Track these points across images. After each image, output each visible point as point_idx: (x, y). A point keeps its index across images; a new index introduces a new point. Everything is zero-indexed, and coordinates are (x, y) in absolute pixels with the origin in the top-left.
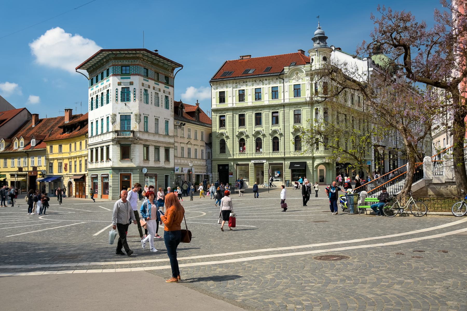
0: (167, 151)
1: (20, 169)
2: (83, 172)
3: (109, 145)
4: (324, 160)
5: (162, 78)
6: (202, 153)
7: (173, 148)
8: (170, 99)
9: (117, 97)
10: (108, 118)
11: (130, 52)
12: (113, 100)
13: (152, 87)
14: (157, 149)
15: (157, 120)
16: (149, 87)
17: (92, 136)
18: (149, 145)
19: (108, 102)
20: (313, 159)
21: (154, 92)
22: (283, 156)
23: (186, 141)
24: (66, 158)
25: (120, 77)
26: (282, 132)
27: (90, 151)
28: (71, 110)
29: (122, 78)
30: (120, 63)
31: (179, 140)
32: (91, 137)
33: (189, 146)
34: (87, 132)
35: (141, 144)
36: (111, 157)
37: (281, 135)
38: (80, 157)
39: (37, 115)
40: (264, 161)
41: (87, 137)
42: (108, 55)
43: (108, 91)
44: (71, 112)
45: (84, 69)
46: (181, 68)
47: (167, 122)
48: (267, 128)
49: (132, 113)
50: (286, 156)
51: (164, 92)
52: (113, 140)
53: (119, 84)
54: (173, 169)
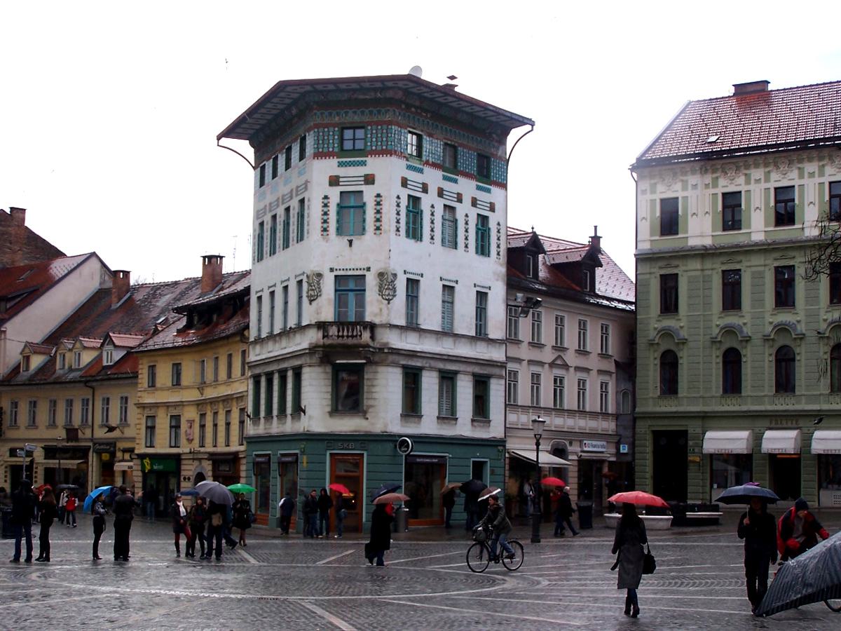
0: (481, 386)
1: (72, 433)
2: (235, 447)
5: (468, 159)
6: (604, 393)
7: (500, 377)
8: (492, 225)
9: (325, 222)
10: (300, 283)
13: (433, 190)
14: (448, 379)
15: (449, 290)
16: (425, 189)
17: (259, 341)
18: (421, 369)
19: (301, 238)
21: (440, 204)
23: (548, 355)
24: (190, 403)
25: (334, 162)
27: (251, 382)
29: (340, 165)
31: (524, 352)
33: (559, 372)
34: (247, 327)
35: (395, 364)
36: (304, 403)
38: (227, 399)
39: (126, 273)
41: (244, 339)
42: (304, 95)
43: (302, 201)
46: (528, 127)
47: (482, 297)
49: (368, 269)
51: (474, 203)
52: (313, 350)
53: (334, 181)
54: (498, 444)
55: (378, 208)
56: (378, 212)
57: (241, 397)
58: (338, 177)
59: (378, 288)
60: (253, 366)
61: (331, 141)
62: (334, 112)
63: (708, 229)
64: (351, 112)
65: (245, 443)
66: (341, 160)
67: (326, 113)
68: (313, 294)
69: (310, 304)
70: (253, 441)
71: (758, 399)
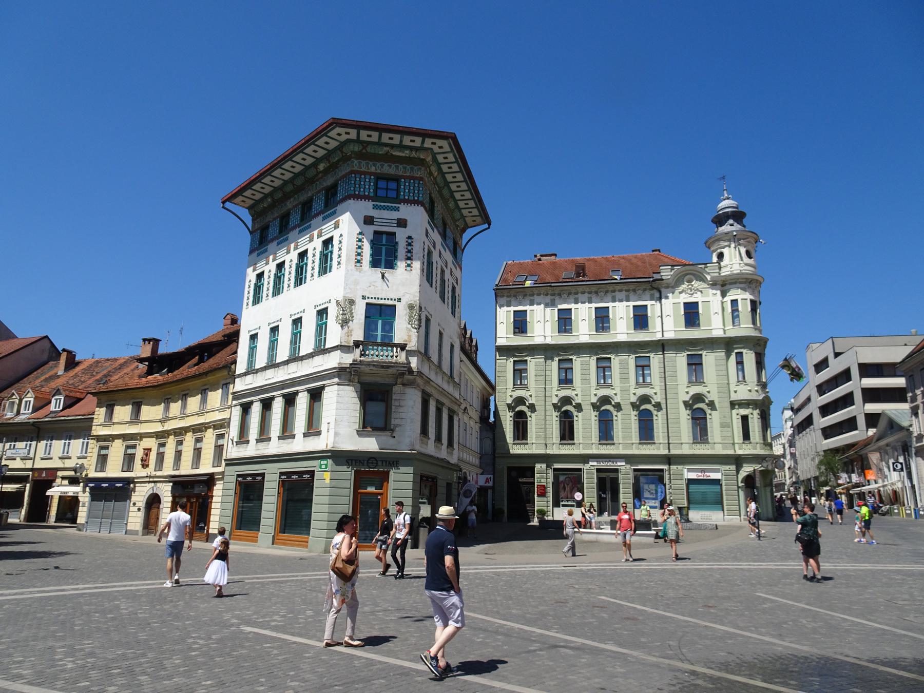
2: (206, 467)
3: (323, 388)
4: (765, 464)
11: (407, 141)
12: (348, 260)
20: (738, 461)
22: (666, 452)
24: (149, 435)
25: (370, 204)
26: (658, 398)
28: (156, 342)
29: (375, 207)
30: (373, 169)
32: (246, 374)
34: (235, 362)
37: (658, 406)
40: (621, 464)
43: (328, 243)
44: (158, 345)
45: (242, 204)
46: (486, 226)
48: (625, 391)
49: (399, 300)
50: (673, 452)
55: (409, 248)
56: (409, 251)
57: (223, 424)
58: (372, 218)
60: (236, 396)
63: (548, 333)
65: (223, 463)
67: (363, 162)
70: (231, 463)
71: (587, 445)
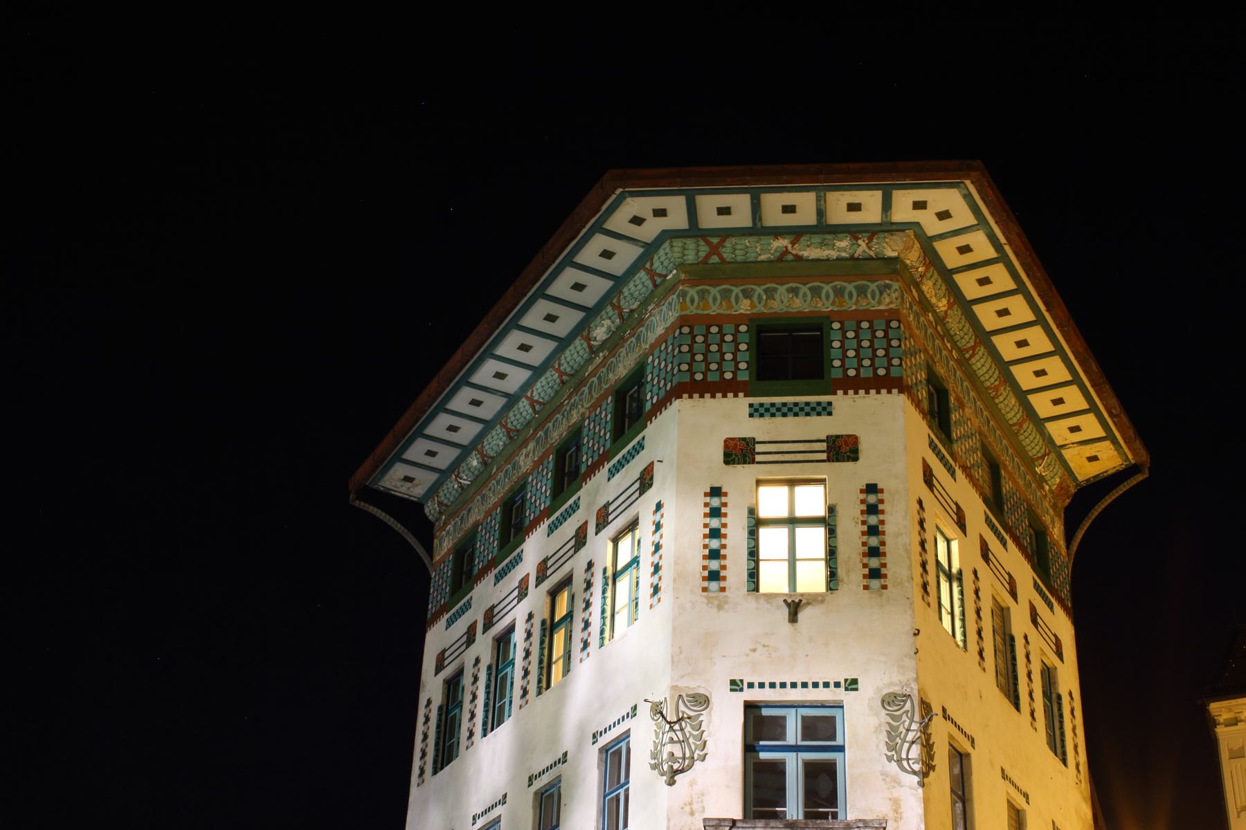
25: (739, 405)
29: (755, 412)
30: (744, 307)
49: (852, 684)
55: (873, 520)
56: (873, 531)
59: (884, 737)
61: (729, 357)
62: (736, 290)
64: (782, 289)
66: (756, 400)
67: (714, 291)
68: (678, 754)
69: (671, 782)
